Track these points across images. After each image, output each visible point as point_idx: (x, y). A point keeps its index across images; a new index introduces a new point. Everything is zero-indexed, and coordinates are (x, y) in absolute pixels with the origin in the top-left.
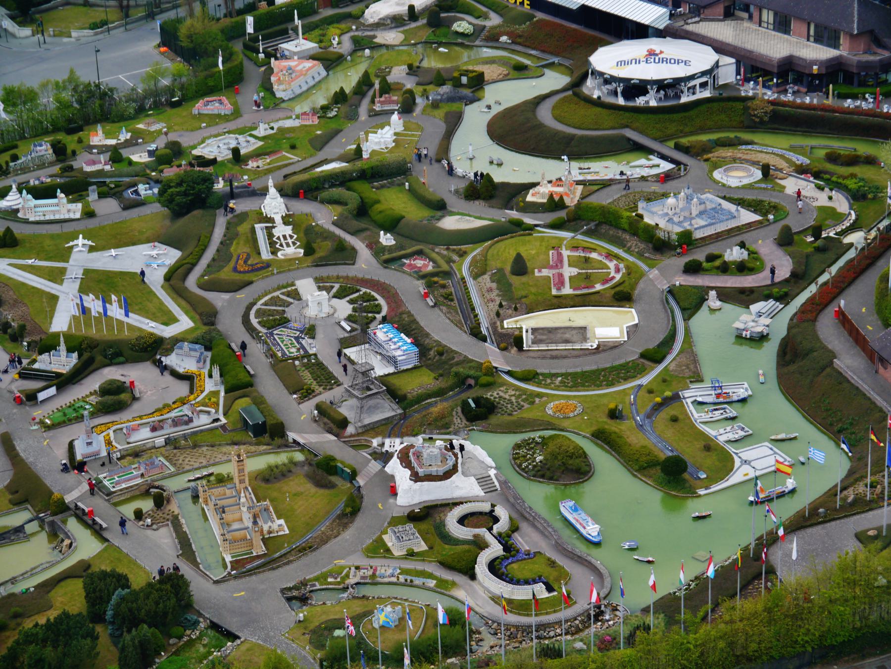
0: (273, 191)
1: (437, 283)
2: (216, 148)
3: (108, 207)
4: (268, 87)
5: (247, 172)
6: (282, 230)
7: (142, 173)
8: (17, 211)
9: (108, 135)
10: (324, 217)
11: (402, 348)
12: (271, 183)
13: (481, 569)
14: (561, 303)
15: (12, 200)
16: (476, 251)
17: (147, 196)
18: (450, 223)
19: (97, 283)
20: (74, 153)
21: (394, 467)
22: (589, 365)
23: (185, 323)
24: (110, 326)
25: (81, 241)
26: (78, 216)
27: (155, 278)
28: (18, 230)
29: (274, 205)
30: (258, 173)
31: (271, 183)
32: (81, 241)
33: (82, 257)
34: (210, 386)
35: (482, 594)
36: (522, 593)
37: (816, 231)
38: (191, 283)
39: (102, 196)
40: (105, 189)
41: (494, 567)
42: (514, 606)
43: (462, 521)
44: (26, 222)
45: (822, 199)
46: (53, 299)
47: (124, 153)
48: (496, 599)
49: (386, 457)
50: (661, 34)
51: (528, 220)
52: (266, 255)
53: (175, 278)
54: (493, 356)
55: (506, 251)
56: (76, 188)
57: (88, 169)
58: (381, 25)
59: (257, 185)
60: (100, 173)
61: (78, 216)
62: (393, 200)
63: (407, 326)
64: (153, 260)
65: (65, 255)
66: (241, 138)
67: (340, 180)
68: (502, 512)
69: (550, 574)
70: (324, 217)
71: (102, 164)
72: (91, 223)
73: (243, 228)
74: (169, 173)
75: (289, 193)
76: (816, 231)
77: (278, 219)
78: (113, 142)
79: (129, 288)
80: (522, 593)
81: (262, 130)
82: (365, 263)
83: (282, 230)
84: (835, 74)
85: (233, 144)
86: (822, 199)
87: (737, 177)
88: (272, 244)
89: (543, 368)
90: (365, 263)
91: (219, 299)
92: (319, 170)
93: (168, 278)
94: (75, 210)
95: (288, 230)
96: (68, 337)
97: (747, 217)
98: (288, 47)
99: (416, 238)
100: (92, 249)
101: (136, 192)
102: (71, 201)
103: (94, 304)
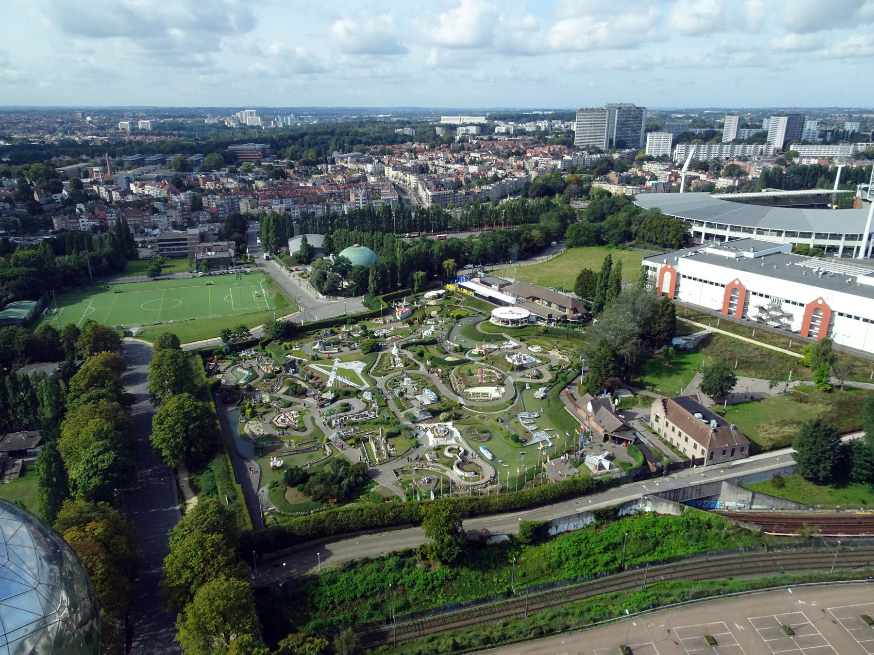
1: (445, 378)
6: (397, 359)
10: (410, 355)
11: (432, 396)
13: (455, 467)
14: (481, 385)
16: (457, 367)
18: (448, 359)
19: (341, 372)
21: (429, 433)
22: (490, 404)
23: (367, 385)
29: (394, 351)
33: (337, 364)
34: (374, 405)
35: (456, 474)
36: (467, 475)
37: (560, 367)
41: (458, 465)
42: (466, 479)
43: (449, 451)
45: (561, 357)
46: (328, 377)
48: (461, 477)
49: (426, 430)
50: (513, 305)
51: (472, 359)
53: (366, 371)
54: (461, 400)
55: (465, 369)
58: (429, 299)
62: (433, 350)
63: (434, 389)
64: (358, 367)
65: (332, 364)
67: (417, 344)
68: (461, 449)
69: (476, 469)
70: (410, 355)
72: (340, 354)
73: (386, 358)
74: (365, 341)
76: (560, 367)
79: (351, 374)
80: (467, 475)
82: (422, 369)
83: (397, 359)
84: (564, 320)
86: (561, 357)
87: (536, 349)
89: (476, 404)
90: (422, 369)
91: (377, 379)
93: (363, 372)
95: (399, 359)
97: (538, 361)
99: (437, 362)
103: (339, 378)
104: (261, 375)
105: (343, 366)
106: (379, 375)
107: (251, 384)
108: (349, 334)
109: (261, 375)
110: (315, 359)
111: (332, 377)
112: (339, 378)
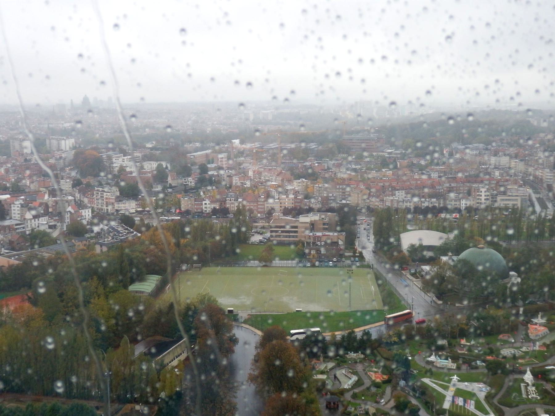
0: (529, 372)
2: (506, 352)
3: (464, 367)
4: (527, 335)
5: (518, 363)
6: (532, 389)
7: (478, 357)
8: (434, 362)
9: (467, 342)
12: (528, 369)
15: (432, 358)
17: (480, 365)
19: (459, 393)
20: (455, 346)
24: (464, 411)
25: (455, 377)
26: (455, 368)
27: (482, 396)
28: (434, 370)
29: (528, 377)
30: (522, 365)
31: (528, 369)
32: (455, 377)
38: (495, 401)
39: (464, 363)
40: (464, 360)
44: (436, 367)
46: (444, 397)
47: (472, 349)
52: (524, 396)
53: (489, 398)
56: (455, 359)
57: (460, 352)
59: (523, 368)
60: (464, 354)
61: (455, 368)
65: (450, 381)
66: (516, 351)
71: (464, 351)
75: (535, 375)
77: (530, 383)
78: (468, 344)
81: (524, 349)
85: (513, 352)
88: (527, 392)
91: (506, 409)
92: (547, 368)
94: (454, 366)
95: (534, 388)
96: (449, 411)
98: (535, 321)
100: (459, 381)
101: (476, 364)
102: (452, 362)
103: (460, 401)
104: (367, 383)
105: (465, 386)
106: (510, 406)
107: (356, 391)
108: (470, 350)
109: (367, 383)
110: (430, 373)
111: (449, 395)
112: (460, 401)
